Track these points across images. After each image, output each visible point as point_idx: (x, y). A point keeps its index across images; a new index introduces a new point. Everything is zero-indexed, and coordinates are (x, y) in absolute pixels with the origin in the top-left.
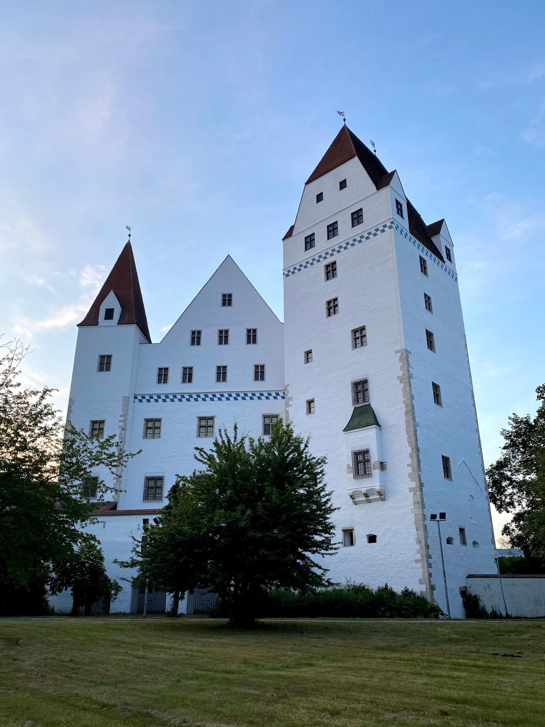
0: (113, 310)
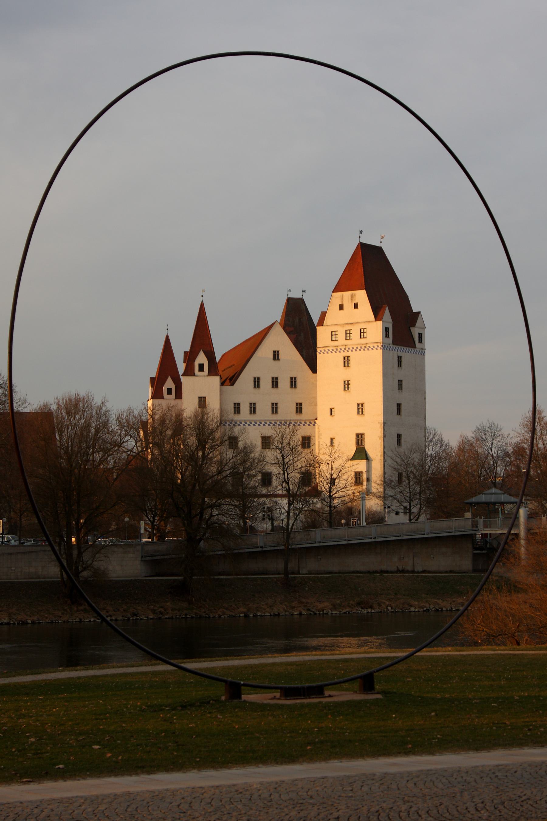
0: (203, 365)
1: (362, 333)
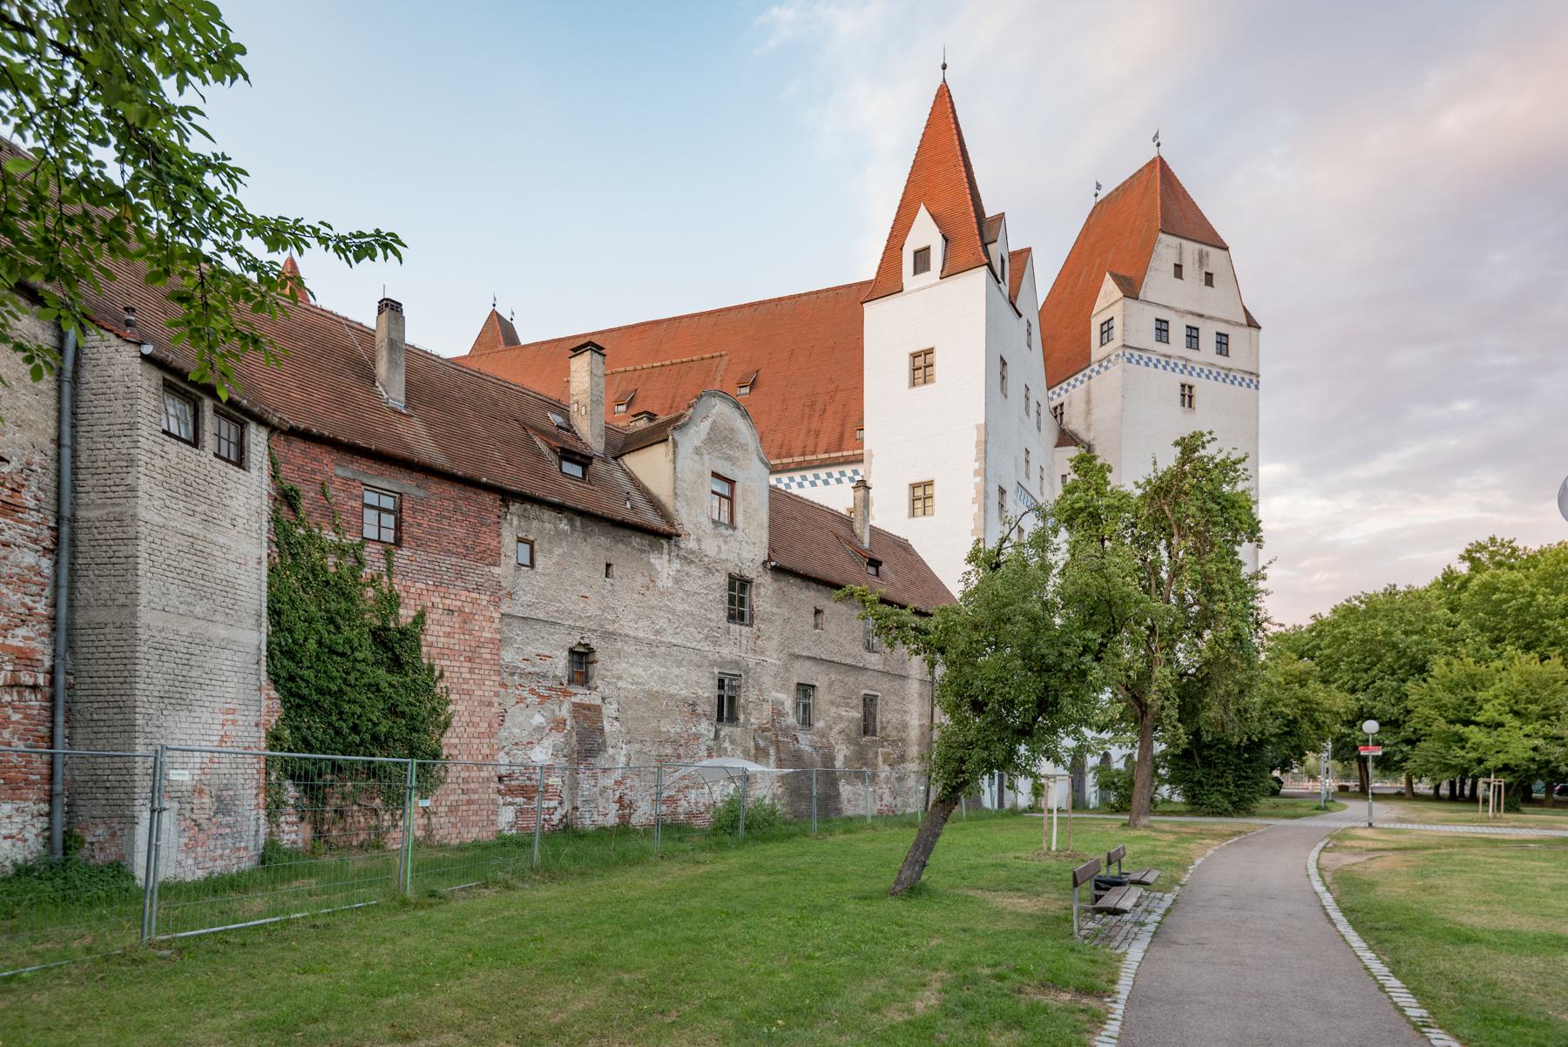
1: (1222, 343)
